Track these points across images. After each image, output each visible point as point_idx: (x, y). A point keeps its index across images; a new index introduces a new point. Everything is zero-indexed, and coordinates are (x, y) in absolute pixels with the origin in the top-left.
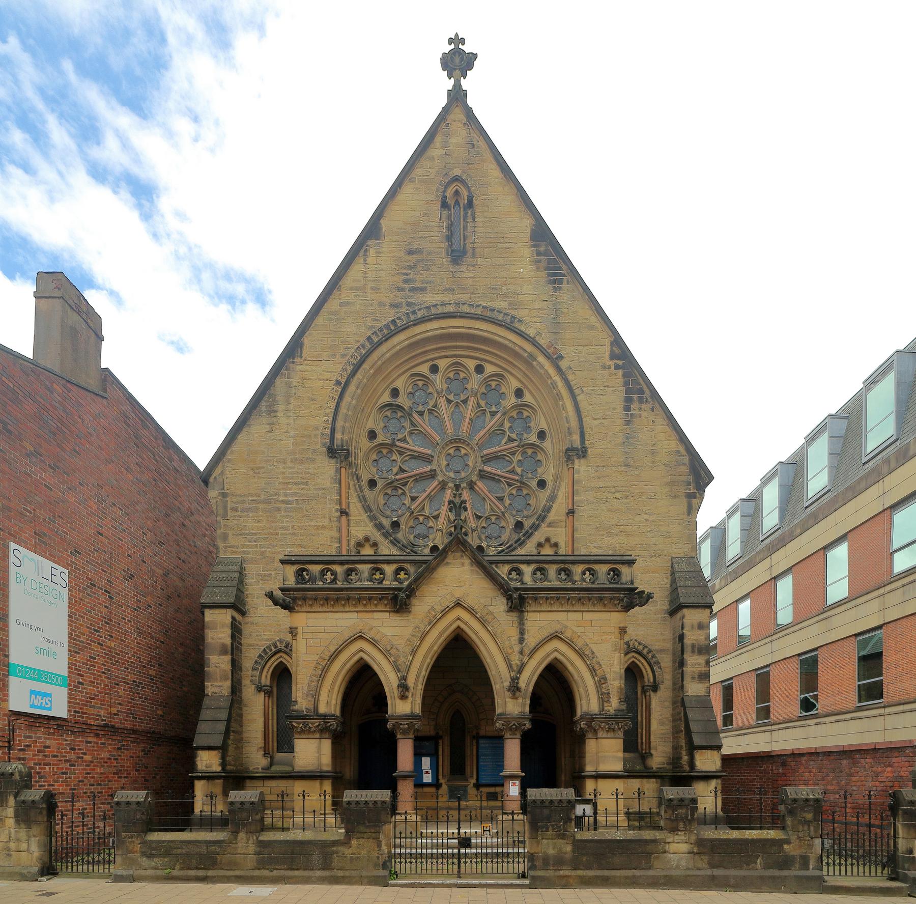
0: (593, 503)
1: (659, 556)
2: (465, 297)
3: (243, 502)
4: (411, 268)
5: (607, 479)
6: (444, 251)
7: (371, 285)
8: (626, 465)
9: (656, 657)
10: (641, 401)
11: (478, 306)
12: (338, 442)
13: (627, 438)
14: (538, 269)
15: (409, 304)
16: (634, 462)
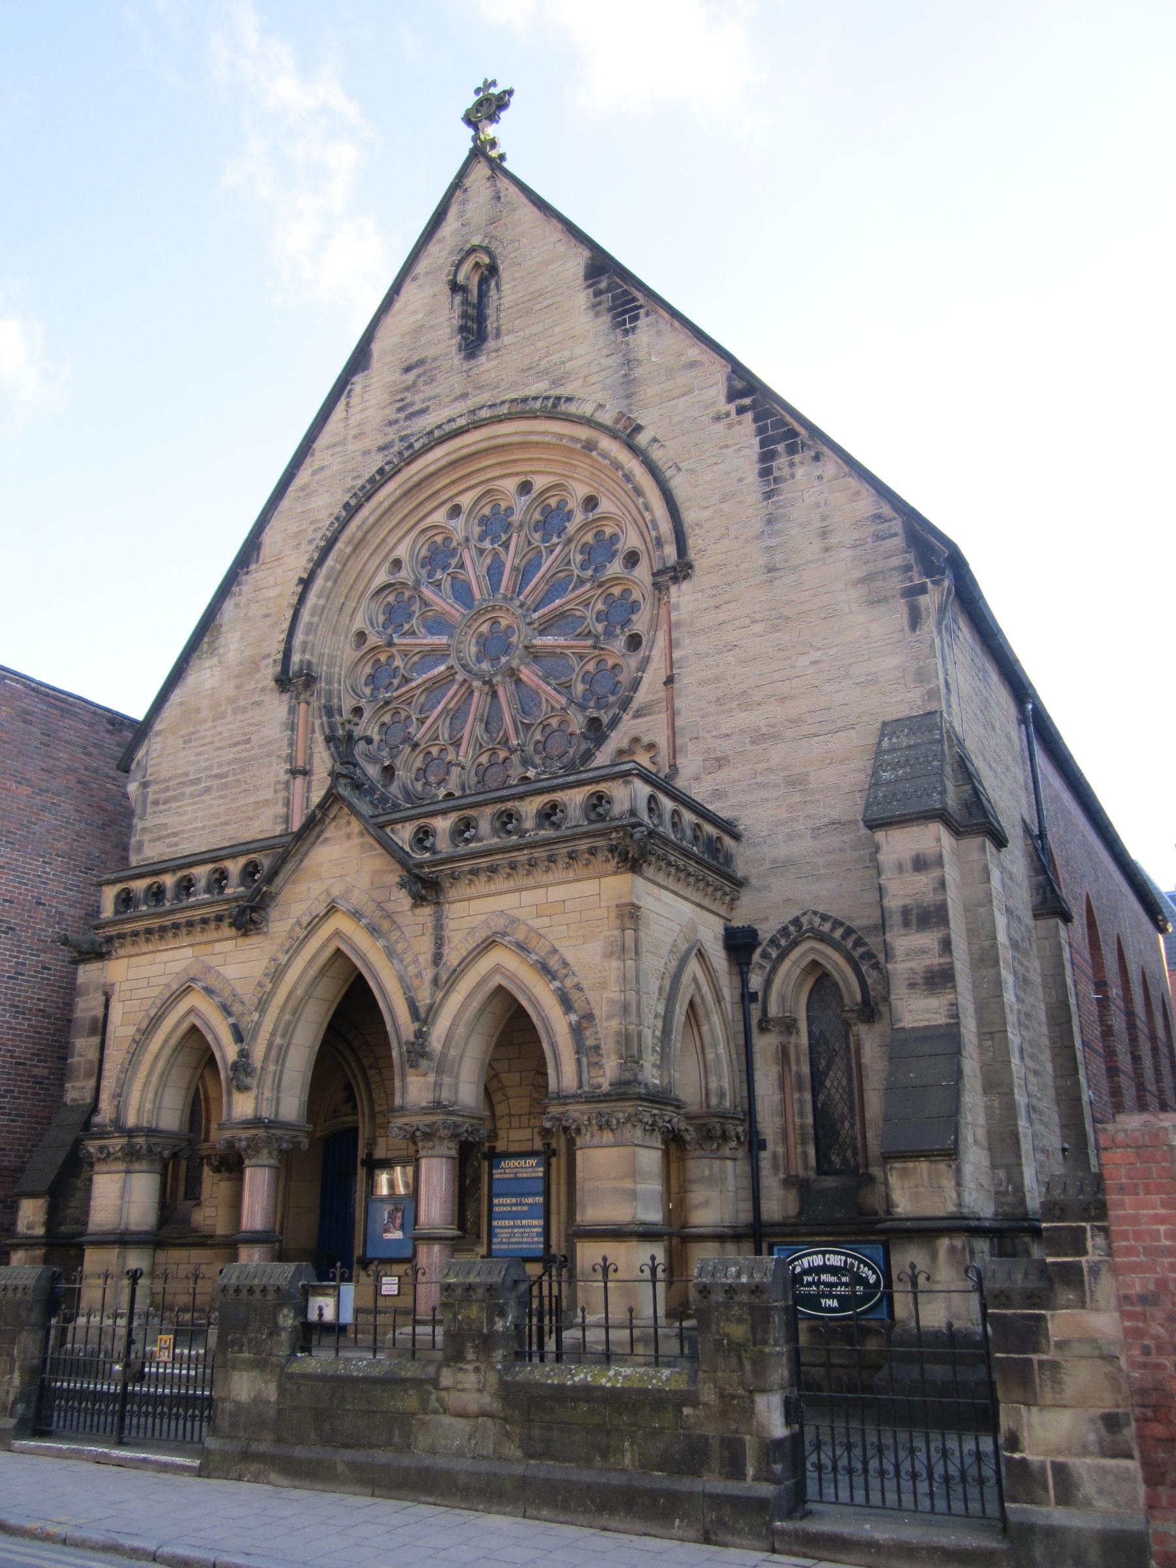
0: (708, 655)
2: (485, 397)
3: (167, 789)
4: (407, 389)
5: (732, 606)
6: (455, 349)
8: (770, 570)
9: (865, 944)
10: (792, 450)
11: (503, 403)
13: (769, 522)
14: (597, 315)
15: (402, 439)
16: (786, 561)
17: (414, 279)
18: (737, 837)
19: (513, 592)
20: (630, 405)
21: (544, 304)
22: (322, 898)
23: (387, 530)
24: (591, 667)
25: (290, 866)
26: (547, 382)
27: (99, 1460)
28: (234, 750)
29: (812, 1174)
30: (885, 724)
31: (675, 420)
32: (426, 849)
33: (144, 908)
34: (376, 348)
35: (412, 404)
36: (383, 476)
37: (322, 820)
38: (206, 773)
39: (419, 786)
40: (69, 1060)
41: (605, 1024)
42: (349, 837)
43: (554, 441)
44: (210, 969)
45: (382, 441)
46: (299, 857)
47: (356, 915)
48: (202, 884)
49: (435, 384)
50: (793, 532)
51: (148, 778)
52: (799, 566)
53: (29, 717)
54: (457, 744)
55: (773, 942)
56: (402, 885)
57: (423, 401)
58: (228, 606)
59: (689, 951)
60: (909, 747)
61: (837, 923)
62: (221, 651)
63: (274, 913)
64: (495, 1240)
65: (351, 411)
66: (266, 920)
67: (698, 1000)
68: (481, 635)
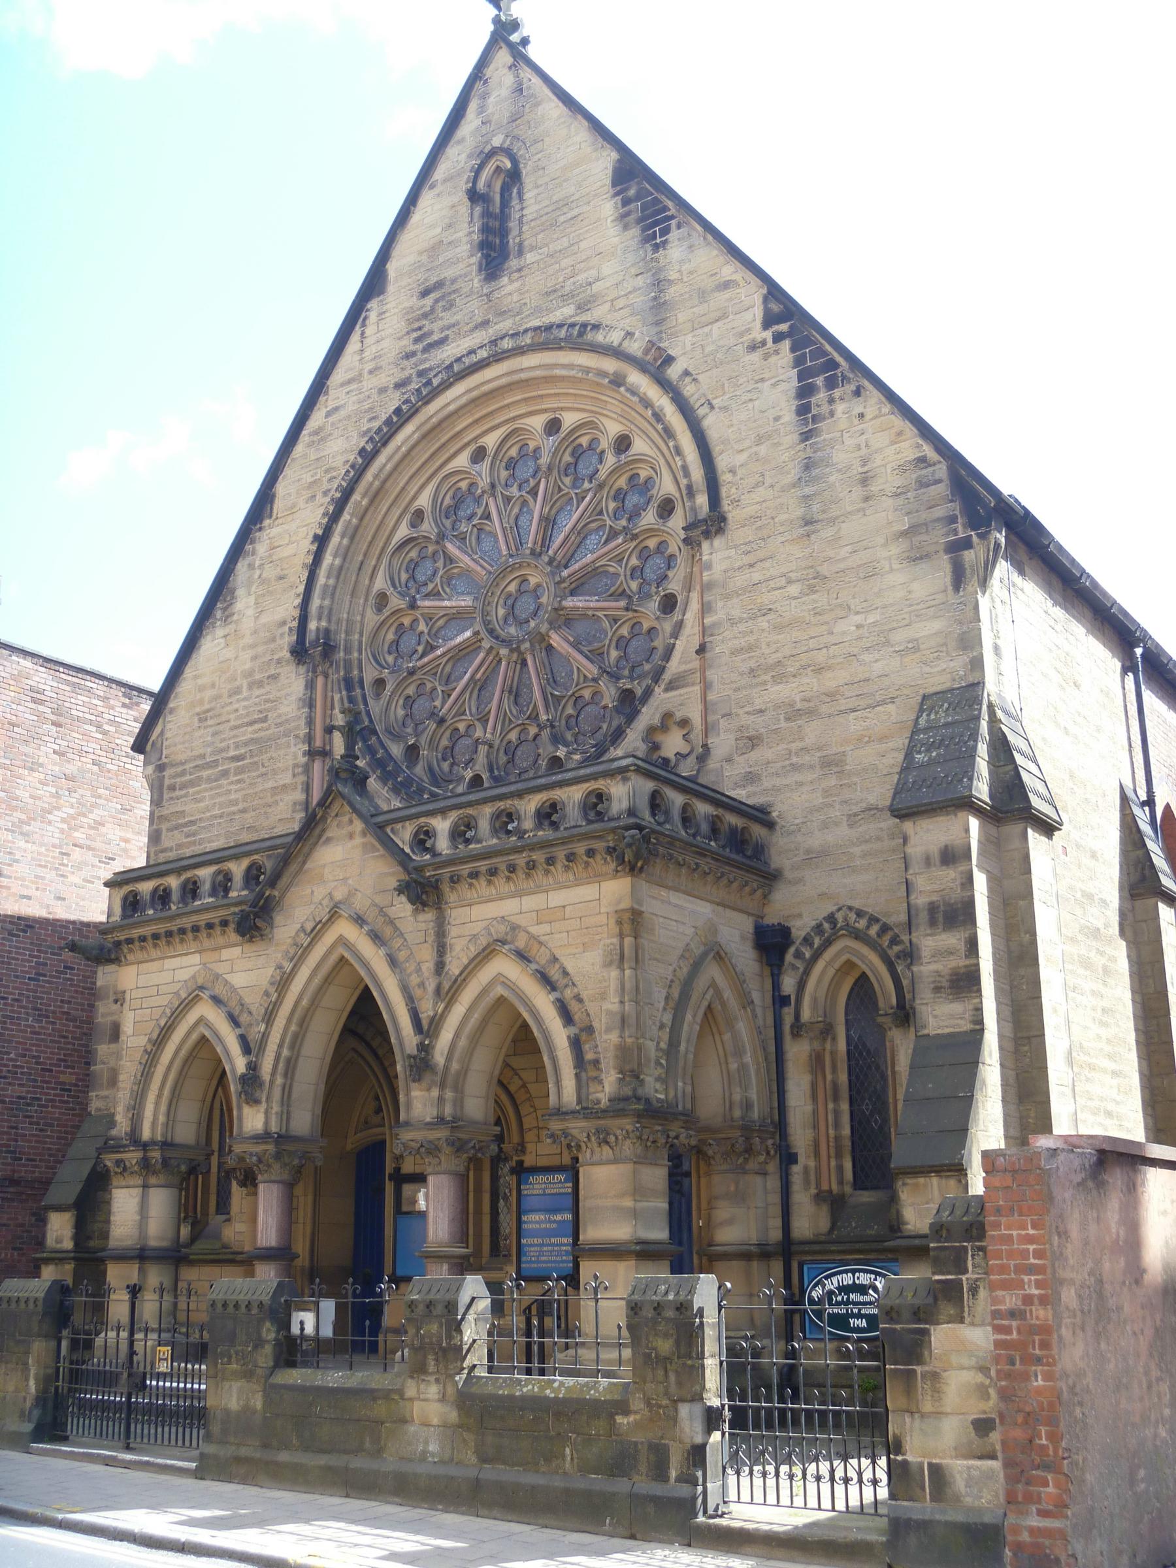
0: (741, 620)
1: (892, 700)
2: (506, 325)
3: (183, 773)
4: (425, 316)
5: (767, 564)
7: (369, 366)
8: (808, 523)
10: (831, 384)
11: (526, 331)
12: (311, 635)
14: (626, 227)
15: (420, 374)
16: (824, 512)
17: (432, 187)
18: (770, 825)
19: (543, 545)
20: (661, 332)
21: (569, 216)
22: (325, 902)
23: (406, 478)
24: (625, 631)
25: (293, 867)
26: (572, 306)
27: (108, 1462)
28: (250, 729)
29: (848, 1189)
30: (924, 697)
31: (708, 349)
32: (427, 850)
33: (151, 912)
34: (392, 268)
35: (431, 333)
36: (400, 417)
37: (324, 818)
38: (224, 755)
39: (446, 766)
40: (92, 1068)
41: (605, 1037)
42: (351, 836)
43: (580, 375)
44: (217, 976)
45: (399, 376)
46: (300, 859)
47: (359, 920)
48: (207, 887)
49: (454, 310)
50: (832, 479)
51: (164, 760)
52: (837, 518)
53: (39, 696)
54: (484, 720)
55: (807, 940)
56: (400, 890)
57: (442, 330)
58: (241, 567)
59: (705, 955)
60: (947, 725)
61: (873, 920)
62: (235, 617)
63: (278, 919)
64: (523, 1259)
65: (367, 341)
66: (270, 922)
67: (717, 1007)
68: (510, 595)
